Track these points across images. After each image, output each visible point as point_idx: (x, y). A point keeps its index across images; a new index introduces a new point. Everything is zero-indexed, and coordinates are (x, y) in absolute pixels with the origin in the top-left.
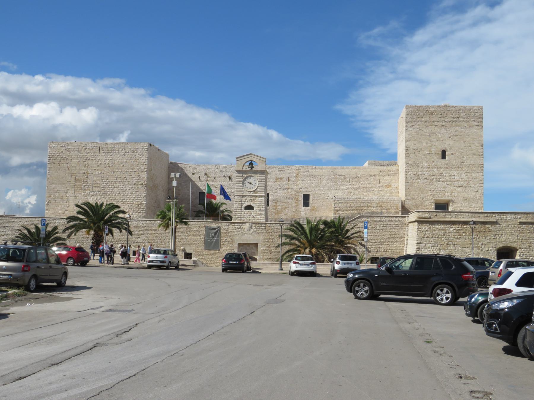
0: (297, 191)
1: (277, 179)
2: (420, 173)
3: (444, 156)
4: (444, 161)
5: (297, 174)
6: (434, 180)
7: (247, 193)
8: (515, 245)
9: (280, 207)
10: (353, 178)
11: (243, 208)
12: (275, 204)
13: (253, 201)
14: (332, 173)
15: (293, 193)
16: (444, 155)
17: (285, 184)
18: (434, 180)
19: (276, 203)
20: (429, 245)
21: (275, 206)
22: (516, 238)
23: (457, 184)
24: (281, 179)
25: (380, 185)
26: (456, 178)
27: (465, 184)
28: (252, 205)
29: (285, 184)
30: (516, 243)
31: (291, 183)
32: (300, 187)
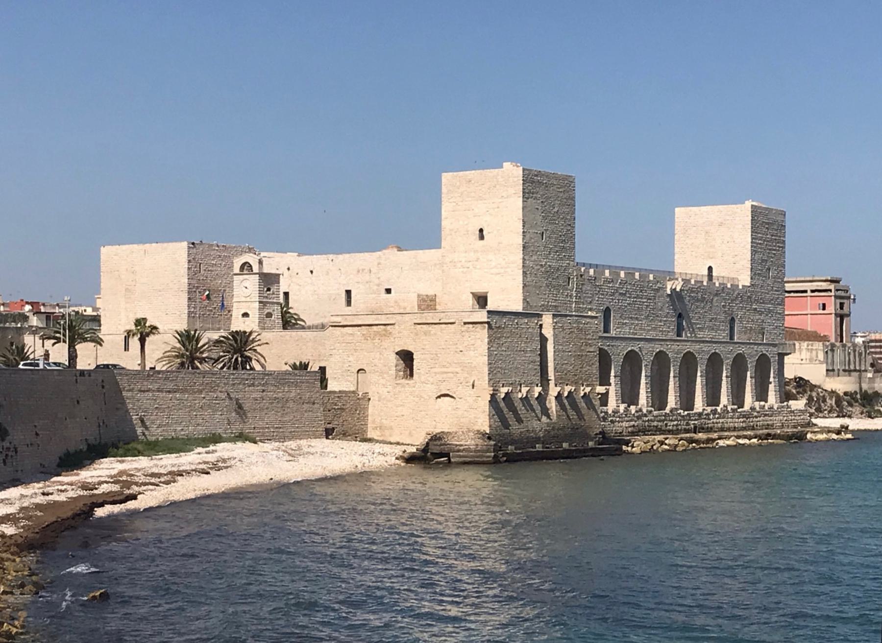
0: (378, 285)
1: (359, 271)
2: (456, 260)
3: (482, 237)
5: (379, 264)
6: (471, 267)
7: (244, 299)
10: (435, 265)
13: (249, 308)
15: (375, 287)
17: (367, 277)
18: (471, 267)
23: (495, 271)
24: (363, 270)
26: (494, 264)
27: (502, 271)
29: (367, 277)
31: (373, 275)
32: (382, 279)
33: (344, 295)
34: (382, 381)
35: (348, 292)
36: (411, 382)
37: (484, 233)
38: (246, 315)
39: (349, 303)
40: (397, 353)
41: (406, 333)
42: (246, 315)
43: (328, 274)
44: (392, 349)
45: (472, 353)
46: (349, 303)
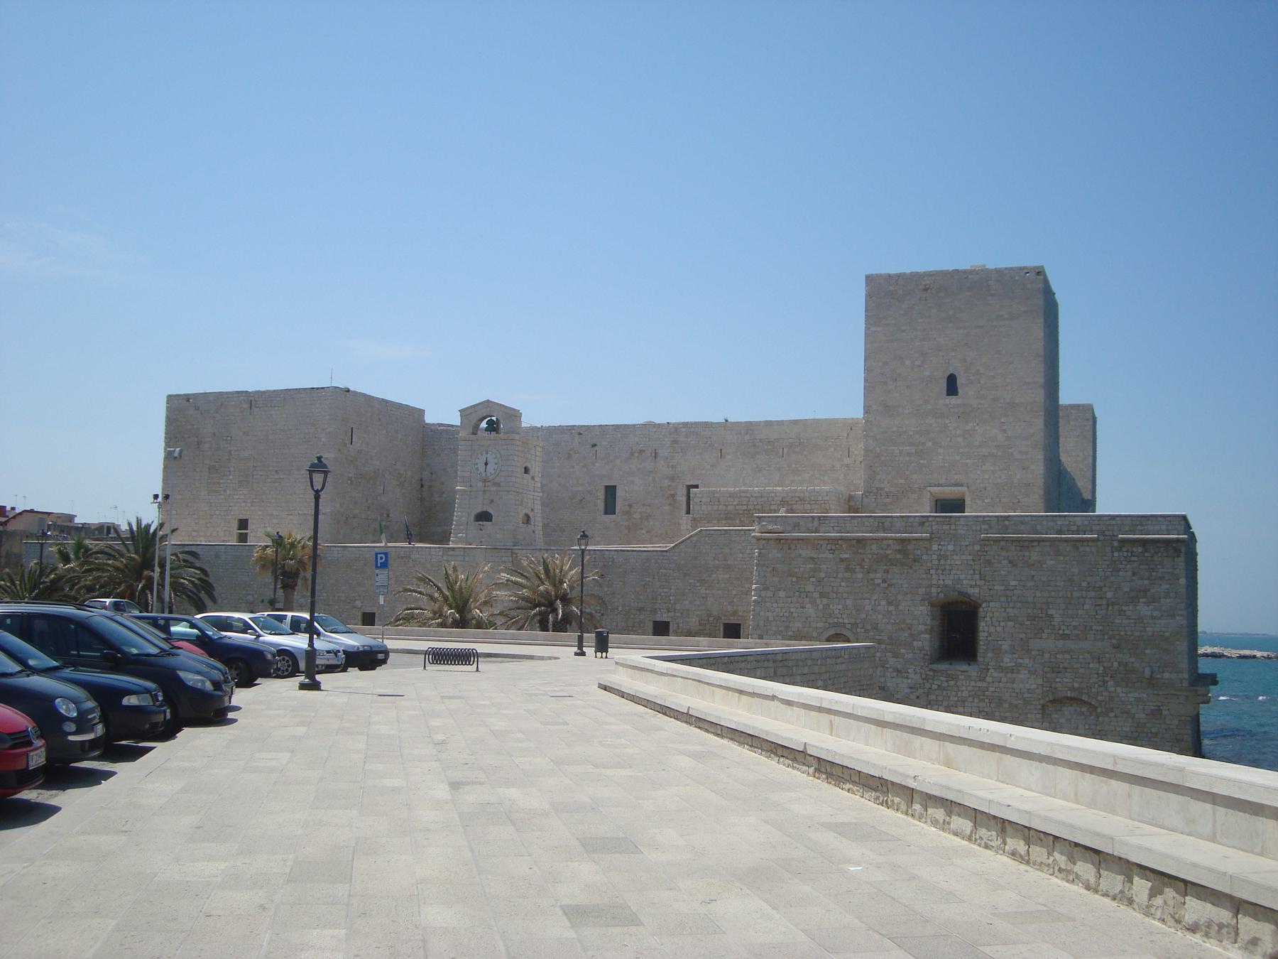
0: (672, 479)
4: (953, 400)
5: (675, 442)
8: (974, 592)
9: (637, 516)
11: (472, 518)
12: (627, 509)
14: (747, 437)
15: (666, 483)
16: (952, 386)
19: (630, 506)
20: (782, 594)
21: (627, 513)
22: (977, 577)
24: (641, 452)
25: (847, 461)
28: (490, 510)
30: (977, 590)
33: (601, 494)
34: (892, 661)
35: (611, 492)
36: (972, 670)
37: (959, 382)
38: (484, 517)
39: (610, 508)
40: (932, 605)
41: (957, 559)
42: (484, 517)
43: (569, 457)
44: (921, 591)
45: (1144, 609)
46: (610, 508)
